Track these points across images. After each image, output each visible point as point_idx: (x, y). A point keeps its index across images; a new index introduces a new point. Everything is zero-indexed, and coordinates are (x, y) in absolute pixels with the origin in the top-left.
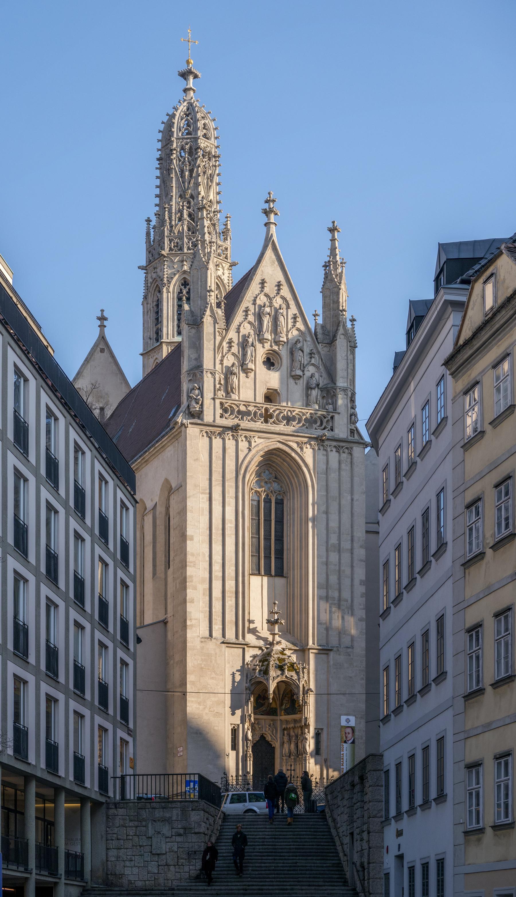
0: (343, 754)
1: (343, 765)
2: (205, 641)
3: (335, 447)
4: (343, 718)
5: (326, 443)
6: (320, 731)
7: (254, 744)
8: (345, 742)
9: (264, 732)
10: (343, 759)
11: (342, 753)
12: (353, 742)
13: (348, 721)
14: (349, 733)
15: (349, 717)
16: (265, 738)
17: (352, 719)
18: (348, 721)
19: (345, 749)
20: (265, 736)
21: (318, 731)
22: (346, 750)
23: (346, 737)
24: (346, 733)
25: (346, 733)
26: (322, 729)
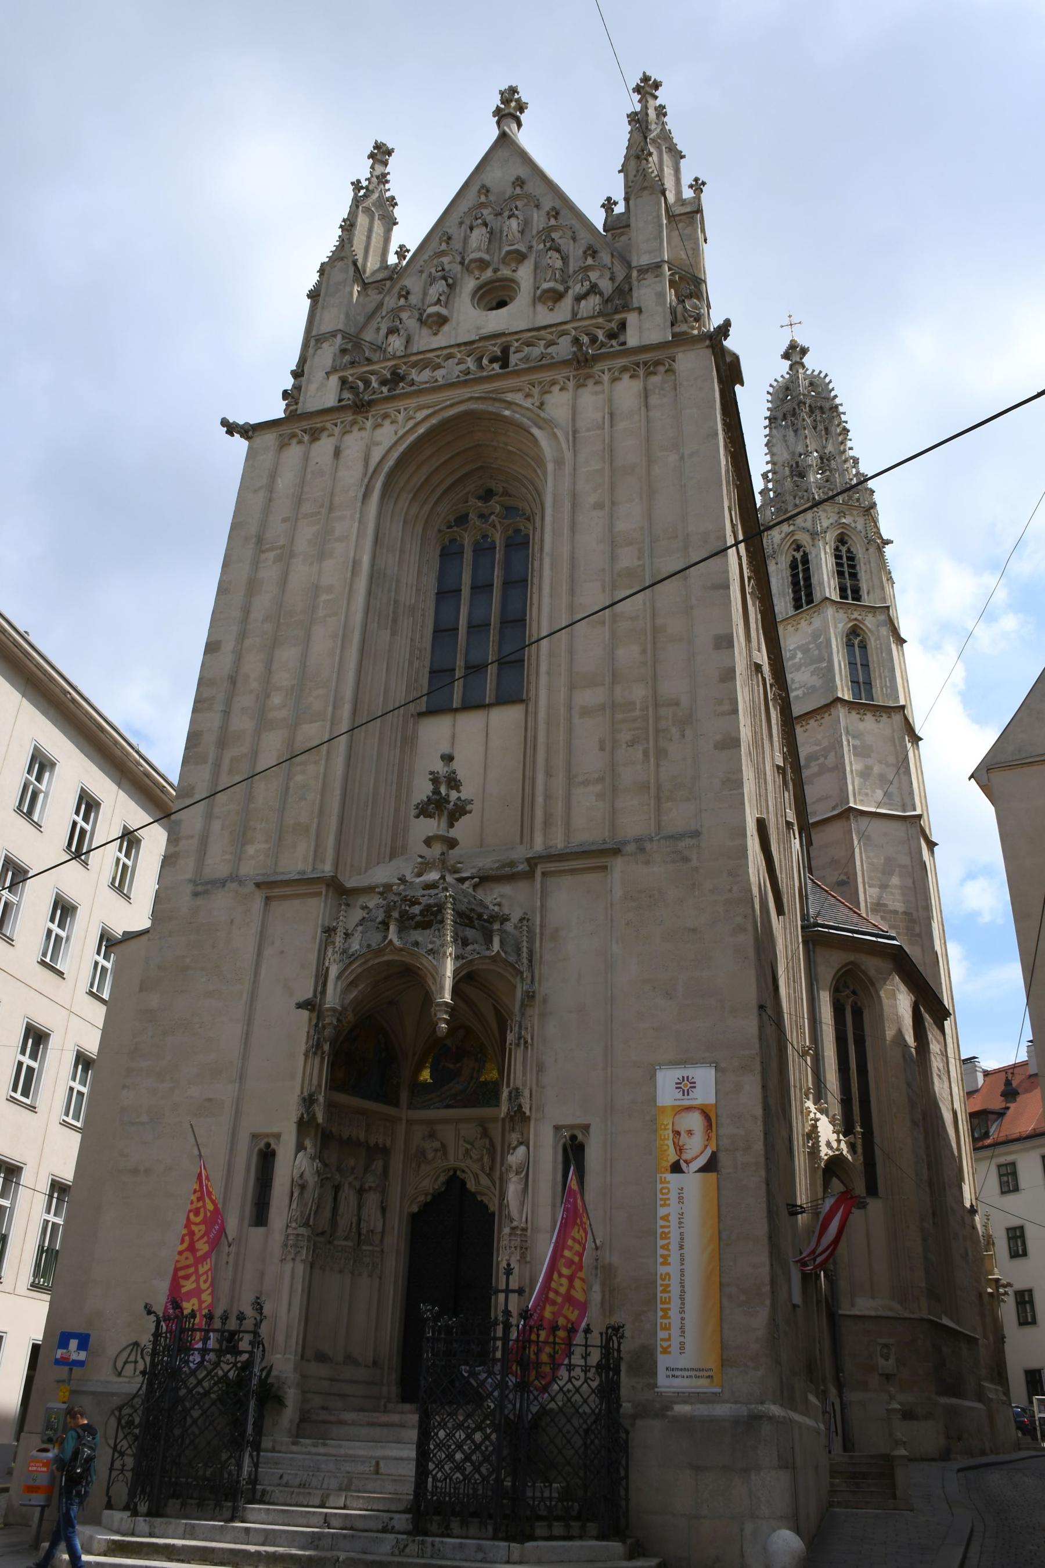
0: (665, 1218)
1: (665, 1263)
2: (206, 892)
3: (624, 369)
4: (667, 1080)
5: (599, 367)
6: (580, 1137)
7: (426, 1207)
8: (676, 1168)
9: (452, 1161)
10: (665, 1236)
11: (662, 1212)
12: (710, 1166)
13: (686, 1086)
14: (690, 1133)
15: (689, 1072)
16: (463, 1183)
17: (705, 1078)
18: (686, 1086)
19: (673, 1196)
20: (462, 1176)
21: (573, 1138)
22: (681, 1200)
23: (680, 1150)
24: (677, 1133)
25: (677, 1133)
26: (586, 1128)
